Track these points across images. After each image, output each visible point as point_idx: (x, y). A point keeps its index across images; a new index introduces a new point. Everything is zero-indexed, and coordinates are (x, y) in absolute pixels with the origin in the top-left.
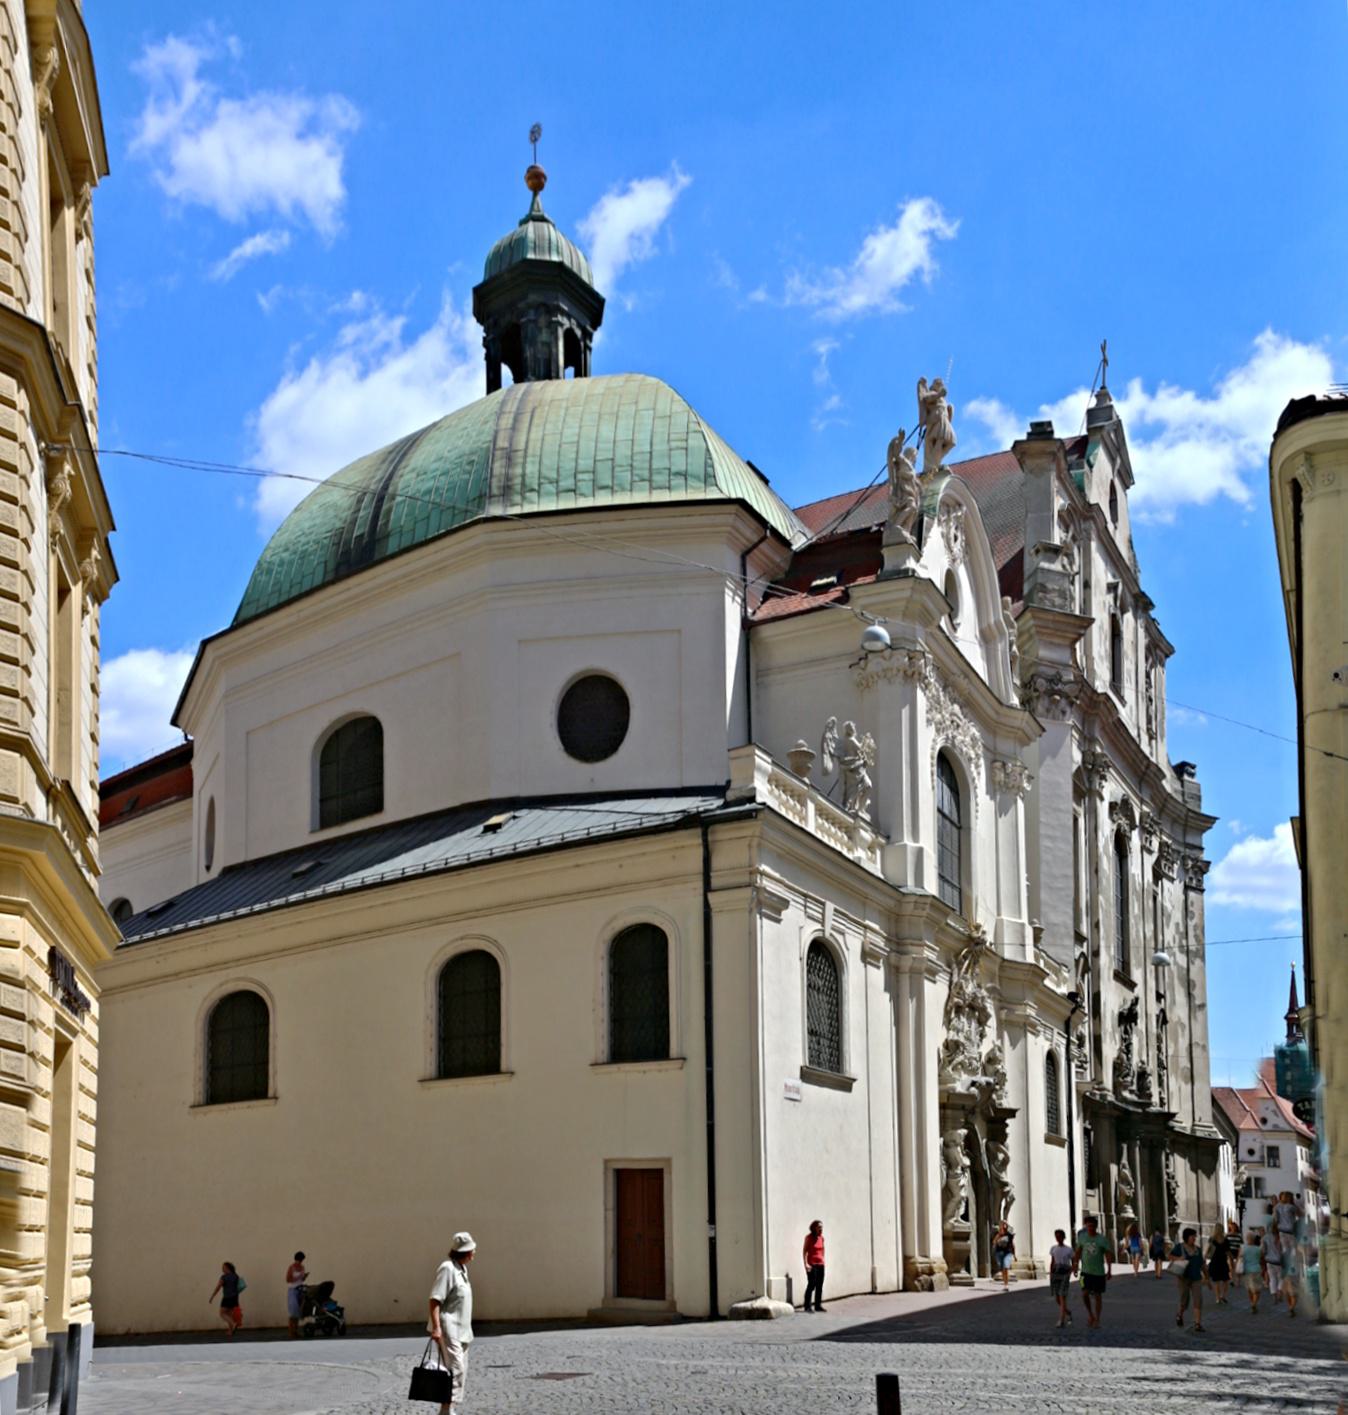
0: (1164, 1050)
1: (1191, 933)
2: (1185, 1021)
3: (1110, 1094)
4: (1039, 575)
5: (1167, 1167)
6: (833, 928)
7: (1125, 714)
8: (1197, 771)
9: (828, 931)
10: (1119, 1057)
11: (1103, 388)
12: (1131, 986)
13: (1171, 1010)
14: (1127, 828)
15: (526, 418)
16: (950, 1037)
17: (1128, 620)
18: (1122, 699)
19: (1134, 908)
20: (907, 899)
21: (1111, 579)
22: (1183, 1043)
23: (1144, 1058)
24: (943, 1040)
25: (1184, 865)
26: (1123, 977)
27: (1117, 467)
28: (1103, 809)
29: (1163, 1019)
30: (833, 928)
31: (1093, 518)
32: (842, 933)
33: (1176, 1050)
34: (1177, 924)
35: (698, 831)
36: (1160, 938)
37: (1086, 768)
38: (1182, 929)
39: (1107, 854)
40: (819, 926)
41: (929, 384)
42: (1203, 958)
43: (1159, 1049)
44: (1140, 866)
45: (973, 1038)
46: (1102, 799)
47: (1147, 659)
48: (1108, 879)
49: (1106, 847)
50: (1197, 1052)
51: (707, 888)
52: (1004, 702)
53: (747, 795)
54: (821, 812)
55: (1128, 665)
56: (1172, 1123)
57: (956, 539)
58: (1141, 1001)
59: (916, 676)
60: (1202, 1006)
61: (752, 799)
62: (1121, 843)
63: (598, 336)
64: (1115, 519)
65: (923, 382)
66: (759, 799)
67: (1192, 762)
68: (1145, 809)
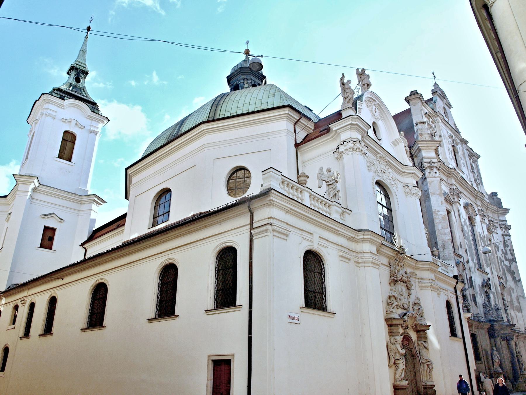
10: (485, 303)
12: (487, 274)
17: (459, 147)
26: (480, 267)
43: (503, 299)
48: (468, 234)
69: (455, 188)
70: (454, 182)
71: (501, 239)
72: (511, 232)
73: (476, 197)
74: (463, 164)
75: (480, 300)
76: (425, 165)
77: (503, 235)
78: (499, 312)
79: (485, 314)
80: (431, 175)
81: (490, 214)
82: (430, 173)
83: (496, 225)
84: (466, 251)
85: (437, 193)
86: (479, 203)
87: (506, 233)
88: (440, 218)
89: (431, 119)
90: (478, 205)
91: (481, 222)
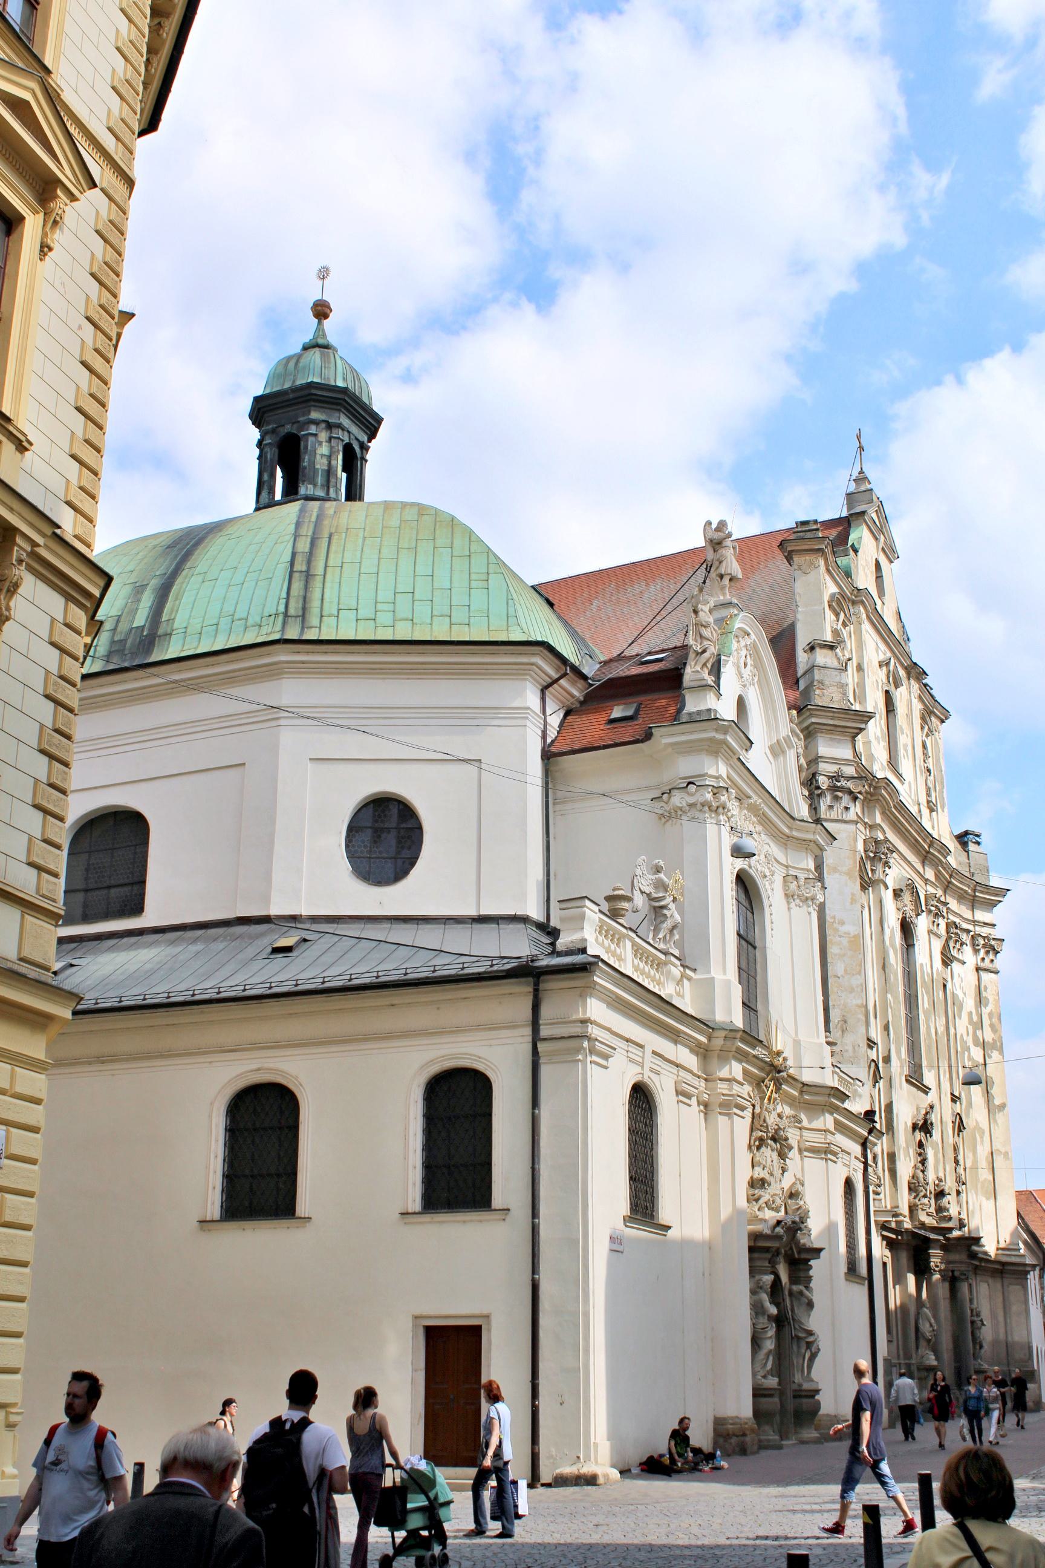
0: (961, 1162)
2: (984, 1125)
3: (907, 1219)
4: (816, 671)
5: (971, 1300)
6: (652, 1070)
8: (983, 839)
9: (647, 1073)
11: (861, 472)
12: (925, 1090)
13: (968, 1115)
14: (913, 914)
15: (324, 543)
16: (756, 1176)
18: (899, 776)
19: (924, 1002)
20: (717, 1034)
21: (882, 657)
22: (983, 1151)
23: (941, 1175)
24: (748, 1178)
25: (974, 945)
26: (915, 1080)
27: (881, 545)
28: (888, 896)
29: (960, 1126)
30: (652, 1070)
31: (862, 602)
32: (658, 1073)
33: (975, 1161)
34: (970, 1013)
35: (531, 979)
36: (952, 1031)
37: (868, 857)
38: (975, 1018)
39: (893, 945)
40: (638, 1069)
41: (714, 526)
43: (957, 1162)
45: (775, 1173)
46: (887, 888)
47: (922, 728)
48: (896, 974)
51: (536, 1039)
52: (796, 816)
53: (580, 946)
54: (637, 951)
55: (903, 740)
56: (975, 1248)
57: (745, 665)
58: (937, 1108)
59: (720, 810)
61: (584, 951)
62: (907, 928)
63: (373, 444)
65: (709, 523)
66: (590, 951)
67: (977, 830)
68: (931, 890)
69: (881, 837)
70: (878, 819)
71: (972, 977)
72: (1000, 962)
73: (926, 858)
74: (905, 746)
75: (905, 1168)
76: (823, 782)
77: (978, 969)
78: (944, 1202)
79: (912, 1209)
80: (833, 815)
81: (953, 904)
82: (831, 807)
83: (964, 937)
84: (886, 1028)
85: (845, 869)
86: (930, 874)
87: (987, 964)
88: (845, 941)
89: (842, 615)
90: (926, 881)
91: (930, 932)
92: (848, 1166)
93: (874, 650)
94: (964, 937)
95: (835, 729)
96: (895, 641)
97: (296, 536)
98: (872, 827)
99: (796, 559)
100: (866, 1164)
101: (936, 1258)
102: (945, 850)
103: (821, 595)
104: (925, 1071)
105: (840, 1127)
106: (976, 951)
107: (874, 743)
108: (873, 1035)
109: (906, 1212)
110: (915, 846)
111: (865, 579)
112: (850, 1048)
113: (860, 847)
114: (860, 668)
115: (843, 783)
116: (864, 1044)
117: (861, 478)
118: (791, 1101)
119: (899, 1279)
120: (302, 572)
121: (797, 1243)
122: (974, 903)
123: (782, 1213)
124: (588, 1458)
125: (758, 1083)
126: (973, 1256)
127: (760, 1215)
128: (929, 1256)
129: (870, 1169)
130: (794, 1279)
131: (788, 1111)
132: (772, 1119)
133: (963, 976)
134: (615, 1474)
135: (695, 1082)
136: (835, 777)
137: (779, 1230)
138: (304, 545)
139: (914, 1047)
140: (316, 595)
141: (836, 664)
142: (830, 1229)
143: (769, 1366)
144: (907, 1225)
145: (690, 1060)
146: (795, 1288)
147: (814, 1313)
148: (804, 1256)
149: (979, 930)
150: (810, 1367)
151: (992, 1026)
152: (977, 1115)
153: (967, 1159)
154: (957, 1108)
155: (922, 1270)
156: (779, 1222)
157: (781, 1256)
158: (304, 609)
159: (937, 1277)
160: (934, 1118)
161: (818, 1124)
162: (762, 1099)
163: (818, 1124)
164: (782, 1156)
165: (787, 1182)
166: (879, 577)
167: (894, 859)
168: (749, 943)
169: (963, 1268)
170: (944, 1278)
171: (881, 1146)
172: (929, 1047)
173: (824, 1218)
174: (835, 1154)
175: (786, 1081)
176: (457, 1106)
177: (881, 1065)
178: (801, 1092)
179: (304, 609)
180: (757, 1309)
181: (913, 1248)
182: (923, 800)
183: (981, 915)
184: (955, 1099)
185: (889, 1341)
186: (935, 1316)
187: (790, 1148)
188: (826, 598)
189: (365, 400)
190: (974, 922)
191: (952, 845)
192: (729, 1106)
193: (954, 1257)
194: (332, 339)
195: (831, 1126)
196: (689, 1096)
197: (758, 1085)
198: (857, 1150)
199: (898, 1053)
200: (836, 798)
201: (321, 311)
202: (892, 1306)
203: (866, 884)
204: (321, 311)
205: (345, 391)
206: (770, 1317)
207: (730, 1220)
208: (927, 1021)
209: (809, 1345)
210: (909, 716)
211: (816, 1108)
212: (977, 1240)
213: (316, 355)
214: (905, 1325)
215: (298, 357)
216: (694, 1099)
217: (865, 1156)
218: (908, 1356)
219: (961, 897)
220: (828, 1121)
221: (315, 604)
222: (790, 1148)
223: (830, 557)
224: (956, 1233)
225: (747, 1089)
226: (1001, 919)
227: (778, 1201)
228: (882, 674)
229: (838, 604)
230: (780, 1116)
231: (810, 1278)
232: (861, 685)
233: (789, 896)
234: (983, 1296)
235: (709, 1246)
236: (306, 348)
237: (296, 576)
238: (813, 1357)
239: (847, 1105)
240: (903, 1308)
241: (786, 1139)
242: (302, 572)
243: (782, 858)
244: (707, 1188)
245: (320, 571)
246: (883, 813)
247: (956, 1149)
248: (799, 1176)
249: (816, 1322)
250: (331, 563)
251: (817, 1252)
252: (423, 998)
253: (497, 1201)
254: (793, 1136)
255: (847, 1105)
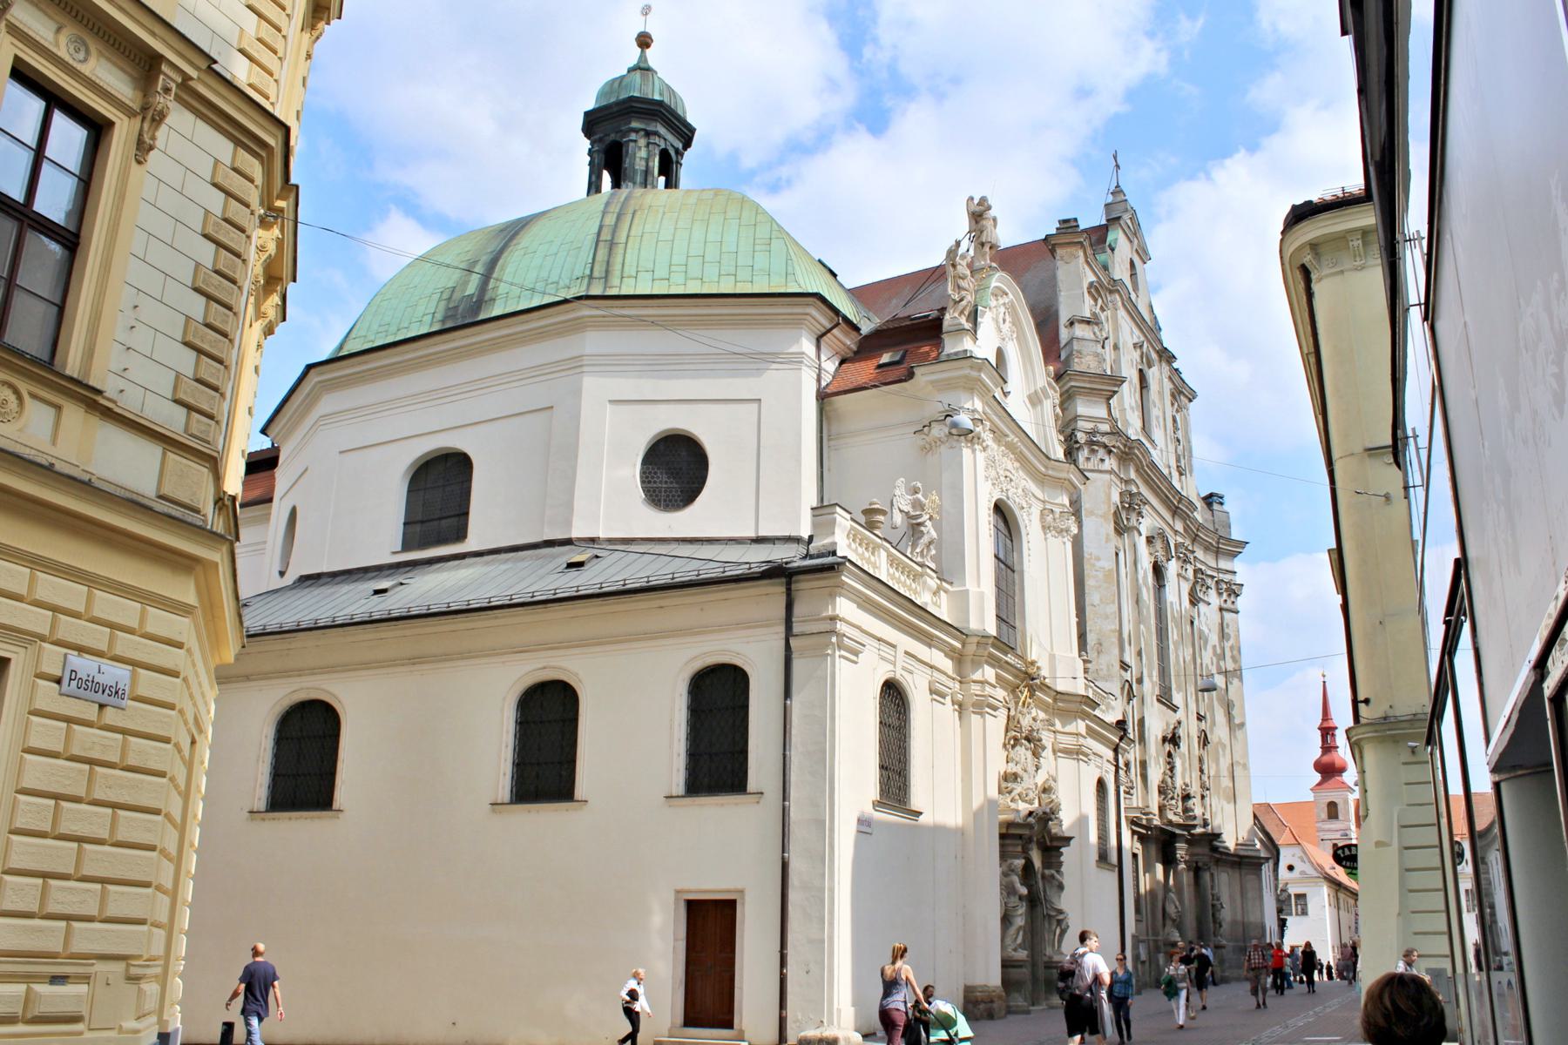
1: (1228, 654)
7: (1156, 455)
12: (1174, 709)
18: (1152, 442)
19: (1173, 635)
22: (1225, 763)
28: (1141, 542)
29: (1204, 741)
33: (1218, 771)
42: (1241, 679)
43: (1202, 771)
44: (1177, 592)
49: (1145, 577)
50: (1238, 771)
55: (1155, 412)
60: (1242, 725)
64: (1136, 288)
69: (1135, 490)
70: (1133, 475)
71: (1216, 617)
72: (1241, 602)
73: (1175, 511)
75: (1156, 774)
77: (1221, 609)
78: (1190, 803)
79: (1162, 809)
80: (1090, 466)
81: (1200, 554)
82: (1088, 459)
83: (1209, 581)
84: (1139, 654)
86: (1179, 526)
87: (1229, 605)
88: (1100, 575)
90: (1176, 532)
91: (1179, 575)
92: (1100, 763)
93: (1129, 334)
94: (1209, 581)
95: (1091, 392)
96: (1150, 329)
97: (604, 213)
98: (1127, 482)
99: (1059, 252)
100: (1117, 767)
101: (1181, 850)
102: (1193, 508)
103: (1081, 281)
104: (1174, 692)
105: (1091, 733)
106: (1220, 594)
107: (1129, 411)
108: (1127, 659)
109: (1156, 811)
110: (1166, 501)
111: (1120, 272)
112: (1104, 667)
113: (1116, 498)
114: (1116, 347)
115: (1098, 438)
116: (1117, 665)
117: (1118, 191)
118: (1044, 707)
119: (1149, 868)
120: (607, 242)
121: (1049, 832)
122: (1218, 553)
123: (1036, 804)
124: (831, 1023)
125: (1014, 690)
126: (1215, 849)
127: (1013, 806)
128: (1175, 849)
129: (1122, 773)
130: (1047, 864)
131: (1042, 715)
132: (1026, 722)
133: (1208, 615)
134: (858, 1037)
135: (950, 683)
136: (1093, 433)
137: (1031, 819)
138: (610, 220)
139: (1164, 672)
140: (618, 260)
141: (1092, 337)
142: (1082, 821)
143: (1020, 940)
144: (1157, 822)
145: (947, 665)
146: (1047, 872)
147: (1064, 894)
148: (1055, 844)
149: (1221, 576)
150: (1060, 942)
151: (1233, 657)
152: (1220, 733)
153: (1211, 769)
154: (1203, 725)
155: (1169, 861)
156: (1031, 813)
157: (1031, 845)
158: (607, 272)
159: (1182, 866)
160: (1181, 732)
161: (1068, 729)
162: (1017, 704)
163: (1070, 728)
164: (1036, 755)
165: (1041, 779)
166: (1133, 275)
167: (1146, 510)
168: (1008, 568)
169: (1206, 859)
170: (1189, 868)
171: (1133, 754)
172: (1178, 675)
173: (1075, 808)
174: (1086, 755)
175: (1041, 690)
176: (718, 699)
177: (1135, 686)
178: (1055, 700)
179: (607, 272)
180: (1008, 890)
181: (1159, 842)
182: (1173, 464)
183: (1223, 564)
184: (1200, 718)
185: (1137, 921)
186: (1181, 900)
187: (1044, 748)
188: (1085, 285)
189: (680, 112)
190: (1218, 570)
191: (1199, 504)
192: (983, 706)
193: (1198, 850)
194: (652, 63)
195: (1083, 731)
196: (943, 696)
197: (1013, 691)
198: (1110, 754)
199: (1150, 676)
200: (1093, 451)
201: (644, 41)
202: (1142, 890)
203: (1120, 530)
204: (644, 41)
205: (660, 103)
206: (1021, 898)
207: (981, 808)
208: (1176, 650)
209: (1059, 922)
210: (1161, 393)
211: (1068, 716)
212: (1217, 836)
213: (637, 75)
214: (1151, 907)
215: (623, 77)
216: (948, 699)
217: (1117, 760)
218: (1156, 933)
219: (1207, 548)
220: (1081, 726)
221: (617, 267)
222: (1044, 748)
223: (1089, 251)
224: (1199, 830)
225: (1001, 693)
226: (1241, 569)
227: (1031, 795)
228: (1136, 355)
229: (1095, 290)
230: (1034, 719)
231: (1061, 864)
232: (1117, 361)
233: (1046, 528)
234: (1224, 883)
235: (960, 832)
236: (630, 70)
237: (601, 245)
238: (1063, 932)
239: (1097, 712)
240: (1152, 893)
241: (1040, 740)
242: (607, 242)
243: (1040, 496)
244: (959, 775)
245: (623, 240)
246: (1137, 471)
247: (1201, 760)
248: (1053, 773)
249: (1067, 902)
250: (633, 233)
251: (1067, 840)
252: (688, 600)
253: (752, 785)
254: (1047, 738)
255: (1097, 712)
